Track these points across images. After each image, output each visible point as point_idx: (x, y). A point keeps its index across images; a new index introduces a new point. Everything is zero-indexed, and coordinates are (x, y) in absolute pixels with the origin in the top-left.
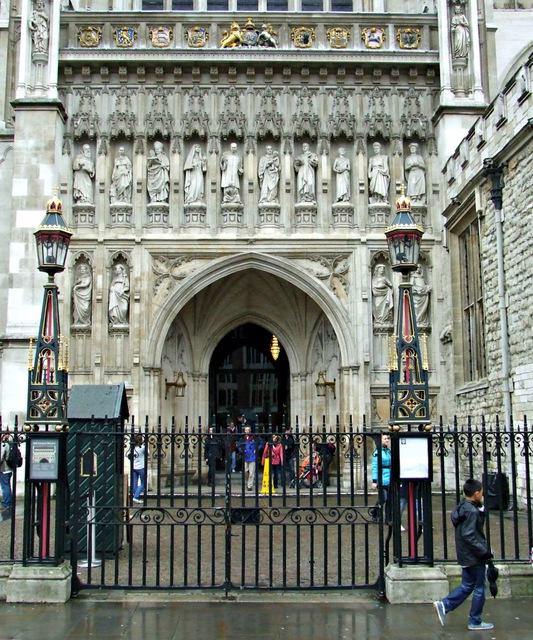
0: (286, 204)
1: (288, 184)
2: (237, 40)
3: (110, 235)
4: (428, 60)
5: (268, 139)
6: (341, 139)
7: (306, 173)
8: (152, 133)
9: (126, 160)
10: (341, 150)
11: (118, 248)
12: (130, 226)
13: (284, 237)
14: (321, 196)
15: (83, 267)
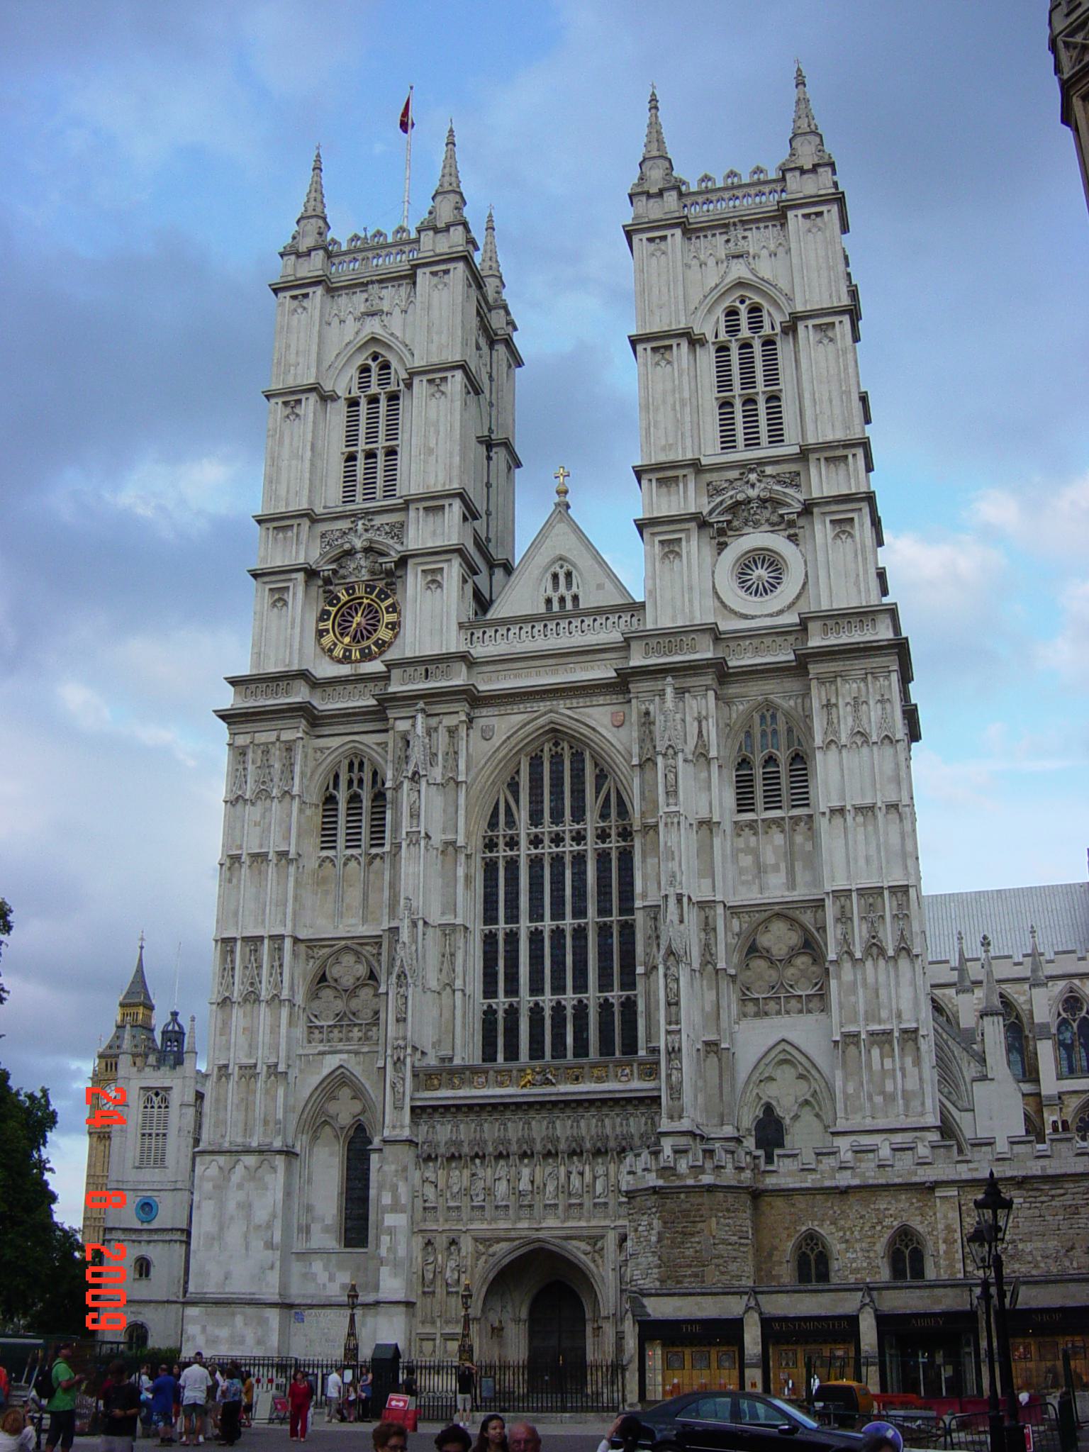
0: (562, 1201)
1: (563, 1187)
2: (529, 1082)
3: (447, 1227)
4: (656, 1094)
5: (548, 1155)
6: (598, 1153)
7: (576, 1181)
8: (473, 1154)
9: (457, 1173)
10: (600, 1160)
11: (452, 1235)
12: (459, 1220)
13: (560, 1225)
14: (585, 1195)
15: (430, 1249)
